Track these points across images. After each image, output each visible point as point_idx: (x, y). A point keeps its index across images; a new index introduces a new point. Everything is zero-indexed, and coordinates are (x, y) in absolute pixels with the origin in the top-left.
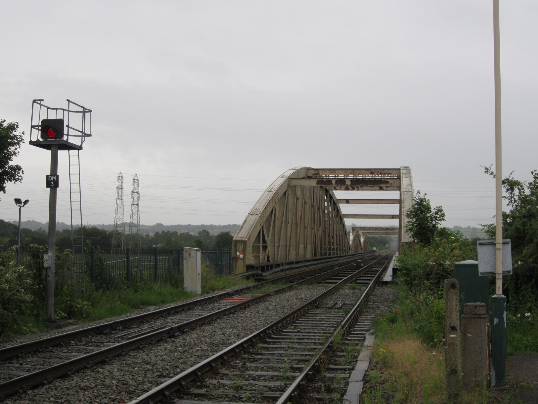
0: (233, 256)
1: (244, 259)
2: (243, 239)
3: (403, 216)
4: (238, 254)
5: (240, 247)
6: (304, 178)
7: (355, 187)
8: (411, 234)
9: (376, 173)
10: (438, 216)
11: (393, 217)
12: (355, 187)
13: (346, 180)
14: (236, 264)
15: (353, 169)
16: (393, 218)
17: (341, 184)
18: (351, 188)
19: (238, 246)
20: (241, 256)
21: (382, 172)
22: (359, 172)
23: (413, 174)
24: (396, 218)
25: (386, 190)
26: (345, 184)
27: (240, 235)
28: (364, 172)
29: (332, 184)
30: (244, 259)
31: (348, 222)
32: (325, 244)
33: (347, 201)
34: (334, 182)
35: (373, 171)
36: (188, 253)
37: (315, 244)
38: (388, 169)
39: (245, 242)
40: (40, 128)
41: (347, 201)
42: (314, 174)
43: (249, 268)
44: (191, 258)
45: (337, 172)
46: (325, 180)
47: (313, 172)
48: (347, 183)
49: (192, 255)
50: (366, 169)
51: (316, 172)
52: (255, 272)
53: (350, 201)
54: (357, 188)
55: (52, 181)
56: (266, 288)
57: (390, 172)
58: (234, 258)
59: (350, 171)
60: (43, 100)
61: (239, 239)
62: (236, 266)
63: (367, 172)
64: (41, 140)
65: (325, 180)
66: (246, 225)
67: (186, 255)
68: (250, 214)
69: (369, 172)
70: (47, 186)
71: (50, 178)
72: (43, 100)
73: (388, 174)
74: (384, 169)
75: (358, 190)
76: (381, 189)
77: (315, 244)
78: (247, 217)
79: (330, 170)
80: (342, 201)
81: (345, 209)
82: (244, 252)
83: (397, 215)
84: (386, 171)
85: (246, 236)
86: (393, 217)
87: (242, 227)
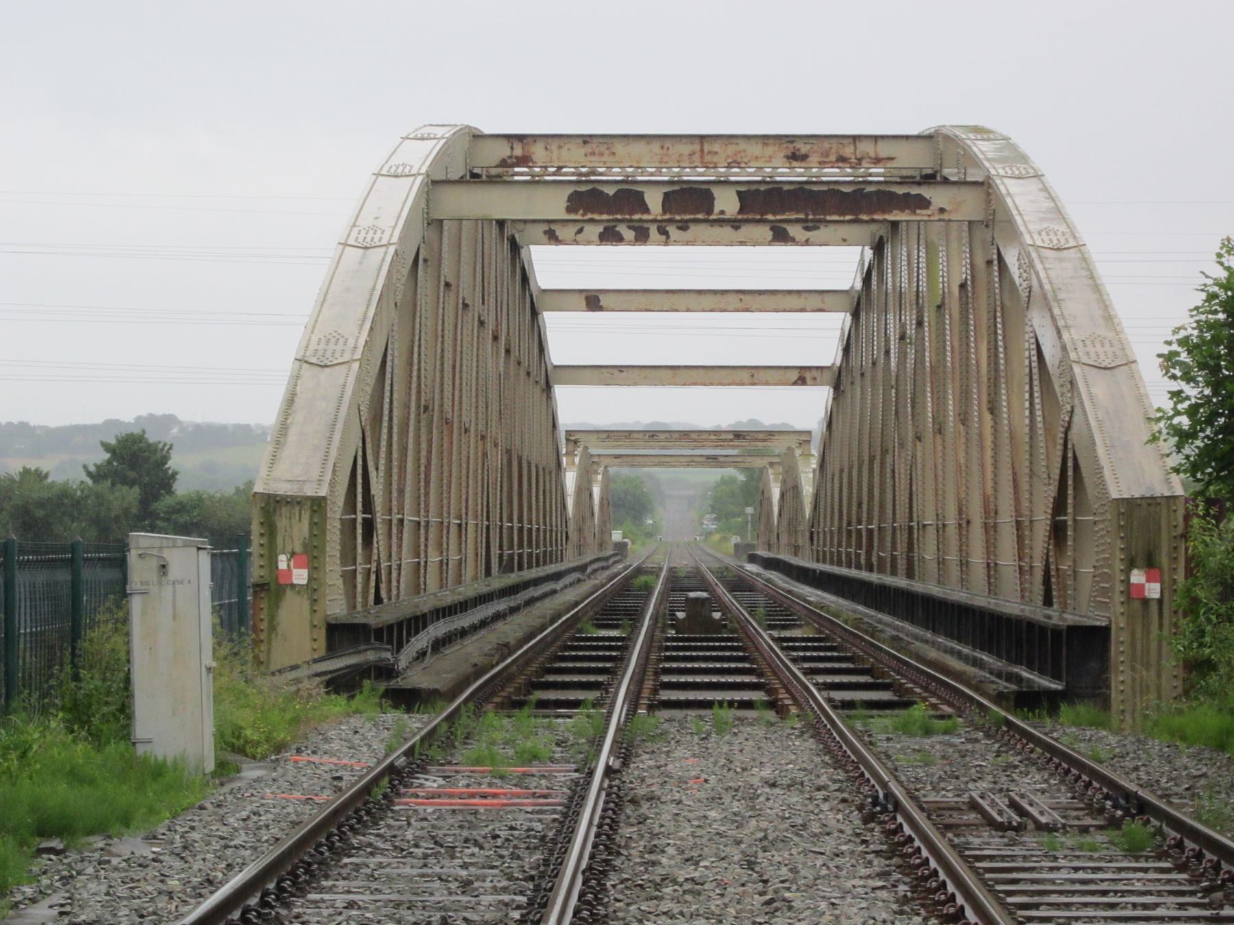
0: (255, 572)
1: (313, 590)
2: (310, 491)
3: (1077, 369)
4: (282, 565)
5: (296, 529)
6: (461, 181)
7: (653, 229)
8: (1176, 460)
9: (814, 159)
11: (803, 376)
12: (653, 229)
13: (717, 192)
14: (272, 618)
15: (702, 138)
16: (801, 381)
17: (610, 208)
18: (629, 234)
19: (282, 522)
20: (300, 576)
21: (848, 151)
22: (731, 149)
23: (1039, 161)
24: (815, 382)
25: (807, 243)
26: (710, 211)
27: (282, 469)
28: (755, 149)
29: (646, 210)
30: (313, 590)
31: (576, 407)
32: (510, 520)
33: (593, 301)
34: (654, 200)
35: (804, 148)
36: (154, 563)
37: (488, 519)
38: (876, 138)
39: (318, 505)
41: (593, 301)
42: (503, 163)
43: (341, 634)
44: (167, 591)
45: (620, 148)
46: (610, 191)
47: (503, 151)
48: (718, 207)
49: (174, 572)
50: (765, 139)
51: (518, 151)
52: (371, 656)
53: (604, 300)
54: (663, 232)
56: (499, 736)
57: (884, 150)
58: (261, 587)
59: (685, 149)
61: (283, 489)
62: (273, 628)
63: (770, 150)
65: (610, 191)
66: (298, 418)
67: (139, 570)
68: (302, 360)
73: (877, 161)
74: (855, 139)
75: (666, 243)
76: (781, 236)
77: (488, 519)
78: (296, 378)
79: (586, 139)
80: (562, 298)
81: (568, 337)
82: (312, 555)
83: (820, 369)
84: (866, 148)
85: (315, 475)
86: (803, 376)
87: (283, 428)
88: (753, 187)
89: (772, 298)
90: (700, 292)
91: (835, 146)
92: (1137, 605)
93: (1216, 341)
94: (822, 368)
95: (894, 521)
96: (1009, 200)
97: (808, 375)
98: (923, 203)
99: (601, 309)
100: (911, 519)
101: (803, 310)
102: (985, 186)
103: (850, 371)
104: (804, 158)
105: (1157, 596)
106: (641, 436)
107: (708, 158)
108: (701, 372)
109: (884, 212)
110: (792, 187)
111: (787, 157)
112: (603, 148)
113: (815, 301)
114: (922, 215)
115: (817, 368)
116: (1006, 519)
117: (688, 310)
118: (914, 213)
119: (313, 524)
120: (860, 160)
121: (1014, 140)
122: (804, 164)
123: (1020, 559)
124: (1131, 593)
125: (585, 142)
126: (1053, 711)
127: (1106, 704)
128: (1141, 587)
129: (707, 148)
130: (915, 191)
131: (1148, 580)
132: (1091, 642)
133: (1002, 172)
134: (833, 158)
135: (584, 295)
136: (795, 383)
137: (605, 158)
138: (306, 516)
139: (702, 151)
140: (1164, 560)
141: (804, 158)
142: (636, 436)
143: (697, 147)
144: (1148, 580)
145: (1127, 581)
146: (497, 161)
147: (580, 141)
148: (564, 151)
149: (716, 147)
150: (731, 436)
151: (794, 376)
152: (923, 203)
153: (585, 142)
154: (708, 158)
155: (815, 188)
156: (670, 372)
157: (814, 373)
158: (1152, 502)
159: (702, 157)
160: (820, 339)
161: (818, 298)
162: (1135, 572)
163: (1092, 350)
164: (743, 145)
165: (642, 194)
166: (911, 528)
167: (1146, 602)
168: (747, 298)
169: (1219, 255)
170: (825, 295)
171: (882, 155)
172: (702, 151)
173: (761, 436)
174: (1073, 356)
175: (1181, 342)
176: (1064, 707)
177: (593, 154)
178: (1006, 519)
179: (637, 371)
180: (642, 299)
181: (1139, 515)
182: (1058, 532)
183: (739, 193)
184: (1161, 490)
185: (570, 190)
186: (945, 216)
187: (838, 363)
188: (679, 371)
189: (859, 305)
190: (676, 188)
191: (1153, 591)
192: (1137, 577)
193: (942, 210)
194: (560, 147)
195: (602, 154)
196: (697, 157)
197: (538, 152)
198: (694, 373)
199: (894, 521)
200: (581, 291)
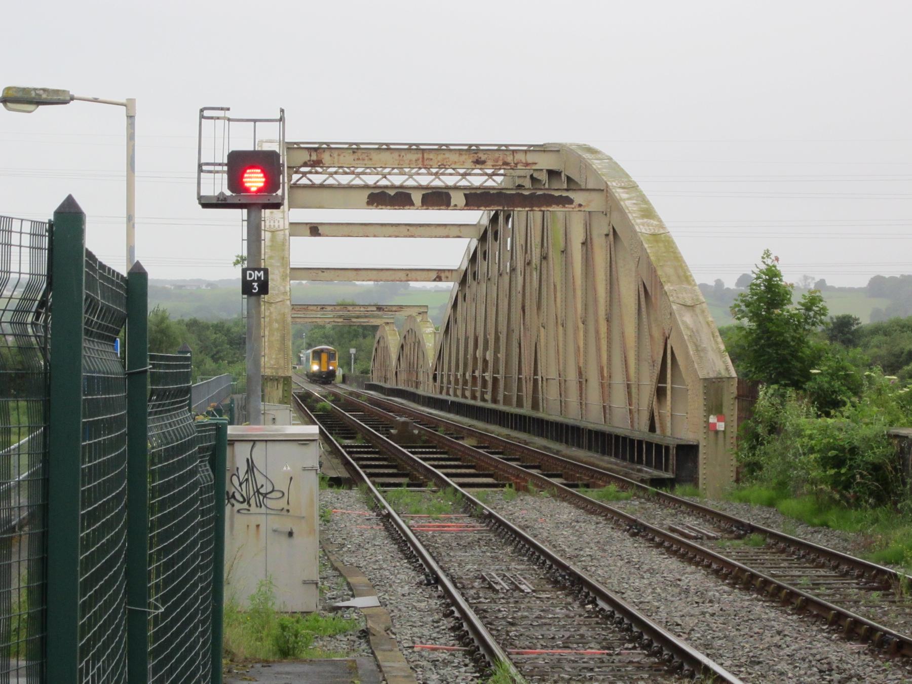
2: (281, 373)
3: (674, 307)
9: (490, 163)
10: (812, 314)
13: (452, 194)
19: (268, 390)
21: (509, 159)
22: (440, 157)
24: (447, 279)
28: (454, 157)
33: (314, 230)
40: (225, 168)
41: (314, 230)
46: (392, 193)
47: (305, 157)
51: (314, 157)
53: (321, 229)
55: (254, 281)
57: (530, 158)
60: (228, 109)
63: (463, 158)
64: (228, 193)
69: (468, 160)
70: (243, 293)
71: (251, 275)
72: (228, 109)
83: (451, 271)
84: (520, 157)
86: (439, 275)
88: (473, 191)
89: (428, 228)
90: (382, 225)
91: (501, 157)
92: (712, 434)
93: (760, 300)
94: (452, 270)
95: (520, 372)
96: (622, 203)
97: (443, 275)
98: (569, 201)
99: (319, 235)
100: (536, 373)
101: (447, 237)
102: (603, 191)
103: (474, 275)
104: (483, 162)
105: (723, 429)
106: (315, 308)
107: (426, 162)
108: (375, 272)
109: (547, 206)
110: (495, 192)
111: (473, 162)
112: (364, 156)
113: (455, 231)
114: (569, 207)
115: (449, 270)
116: (618, 380)
117: (375, 236)
118: (564, 206)
119: (284, 390)
120: (516, 164)
121: (615, 159)
122: (483, 167)
123: (630, 405)
124: (710, 428)
125: (354, 152)
126: (672, 488)
127: (696, 484)
128: (715, 425)
129: (426, 156)
130: (565, 194)
131: (718, 421)
132: (688, 452)
133: (614, 184)
134: (500, 163)
135: (308, 226)
136: (435, 280)
137: (366, 162)
138: (281, 387)
139: (423, 158)
140: (725, 410)
141: (483, 162)
142: (311, 308)
143: (420, 156)
144: (718, 421)
145: (707, 422)
146: (301, 163)
147: (351, 151)
148: (342, 157)
149: (431, 156)
150: (375, 309)
151: (434, 275)
152: (569, 201)
153: (354, 152)
154: (426, 162)
155: (508, 192)
156: (354, 273)
157: (447, 274)
158: (720, 379)
159: (423, 161)
160: (453, 253)
161: (457, 229)
162: (712, 416)
163: (680, 295)
164: (447, 155)
165: (409, 196)
166: (536, 381)
167: (717, 432)
168: (411, 228)
169: (763, 258)
170: (462, 228)
171: (530, 161)
172: (423, 158)
173: (394, 309)
174: (671, 299)
175: (742, 301)
176: (677, 486)
177: (358, 159)
178: (618, 380)
179: (333, 272)
180: (346, 230)
181: (713, 386)
182: (660, 393)
183: (465, 195)
184: (724, 374)
185: (369, 192)
186: (582, 209)
187: (464, 268)
188: (360, 272)
189: (487, 236)
190: (430, 191)
191: (721, 426)
192: (713, 419)
193: (580, 205)
194: (339, 155)
195: (364, 160)
196: (420, 162)
197: (326, 157)
198: (369, 272)
199: (520, 372)
200: (307, 224)
